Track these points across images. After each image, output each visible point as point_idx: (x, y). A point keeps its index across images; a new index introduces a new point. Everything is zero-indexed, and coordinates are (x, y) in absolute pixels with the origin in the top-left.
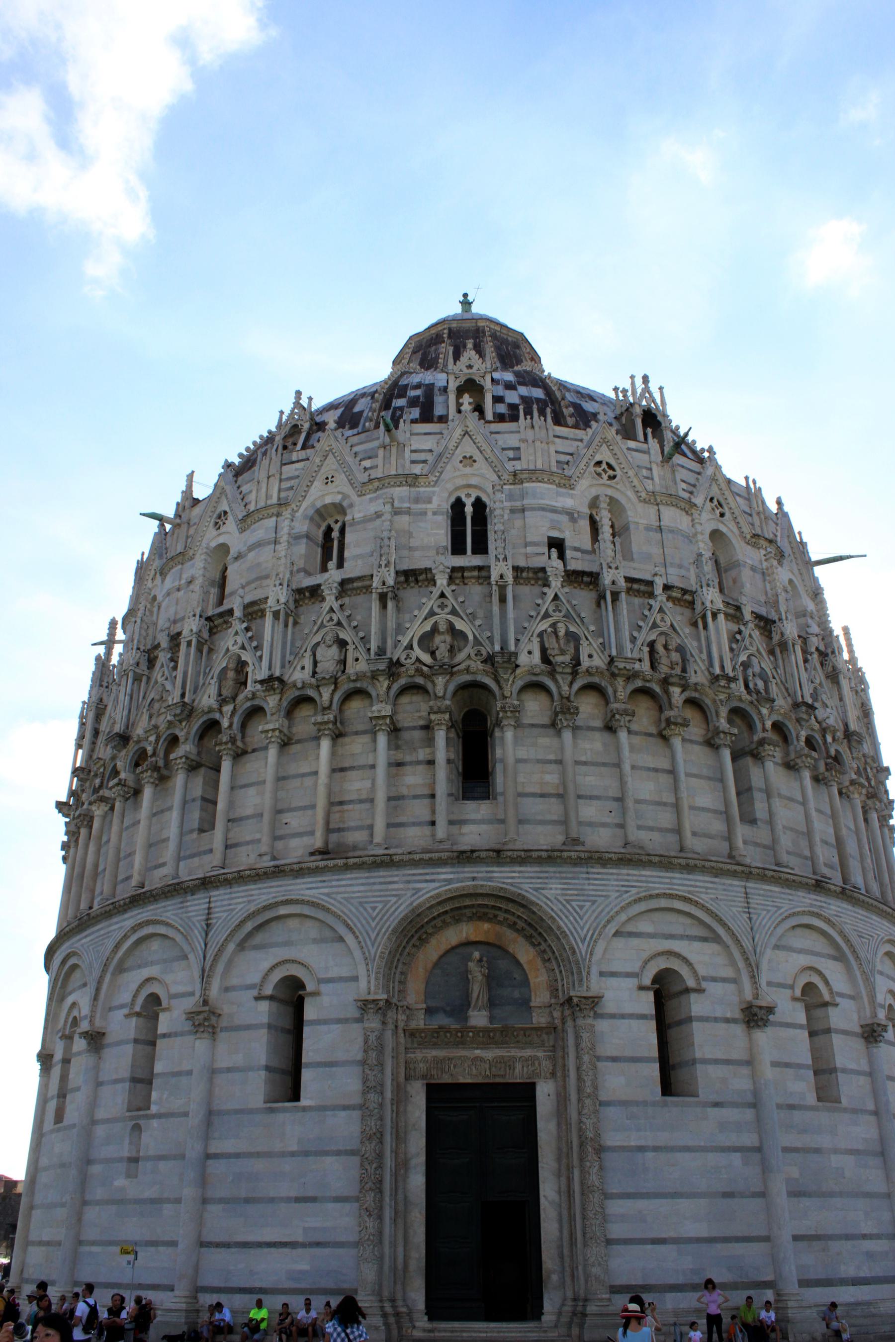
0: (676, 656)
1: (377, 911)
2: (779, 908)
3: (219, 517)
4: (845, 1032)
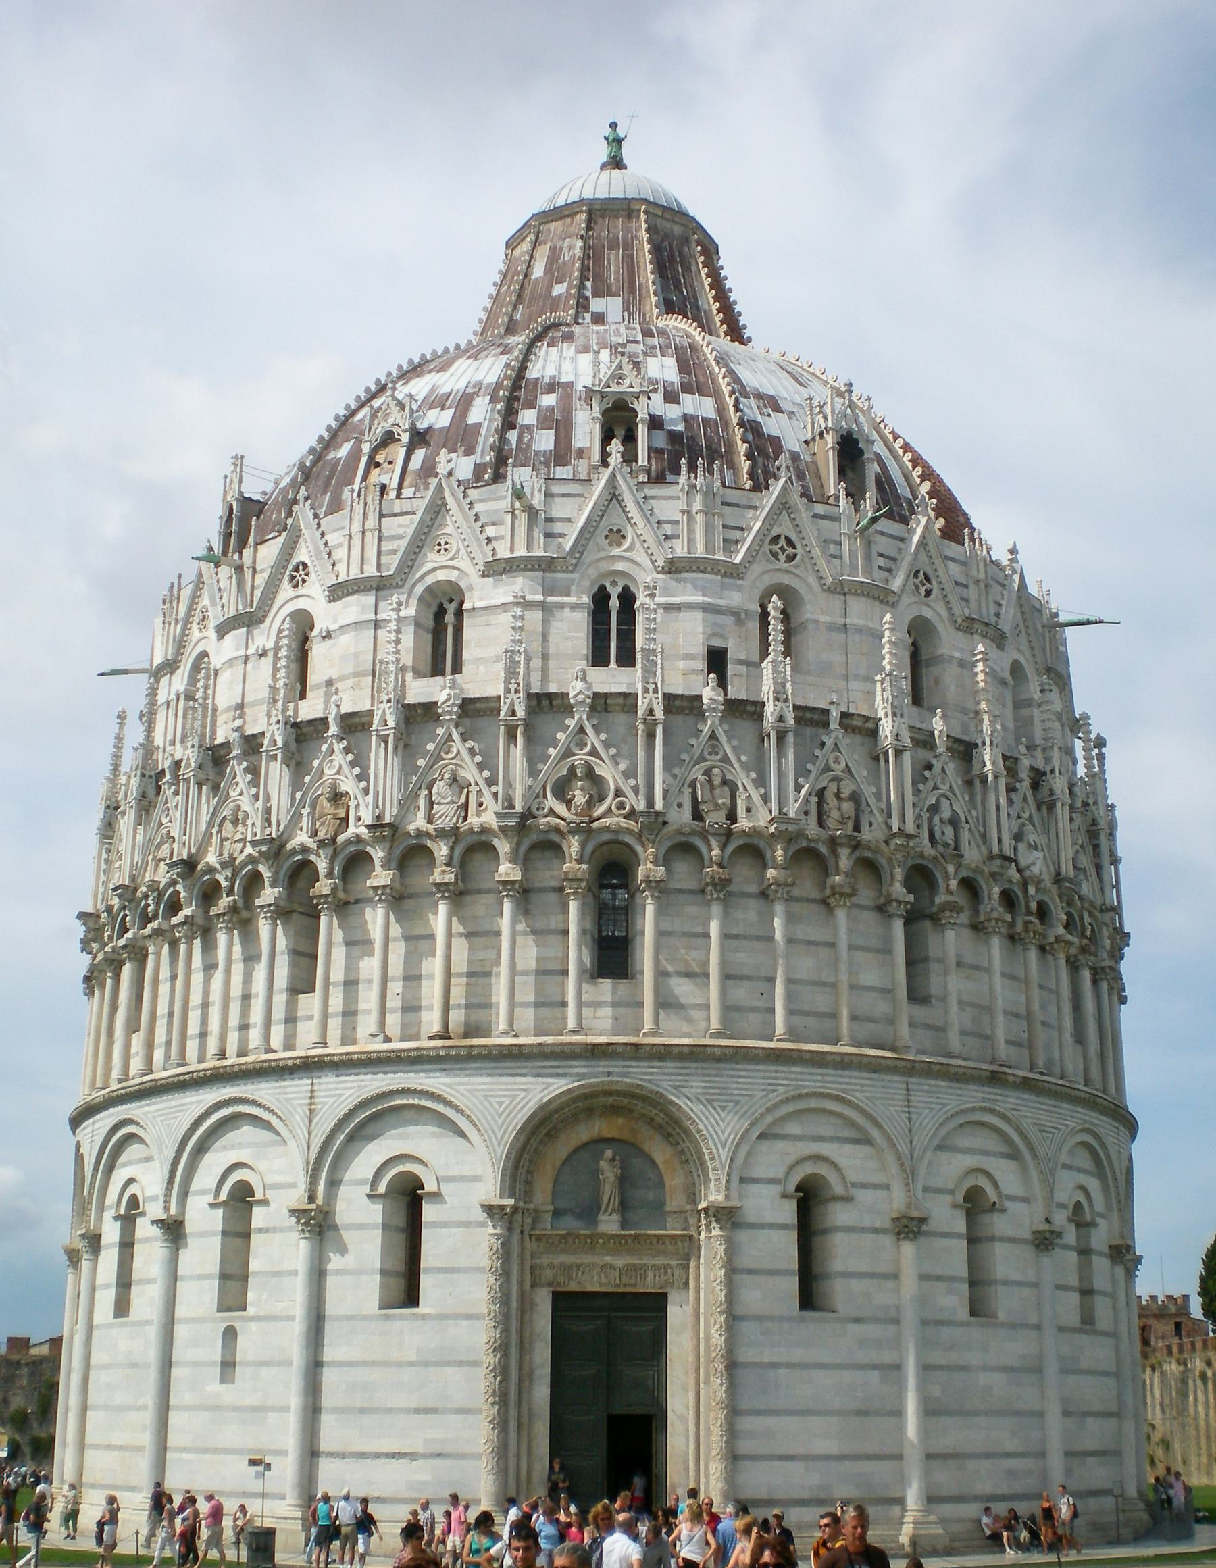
0: (848, 807)
2: (944, 1105)
3: (296, 569)
4: (1012, 1240)
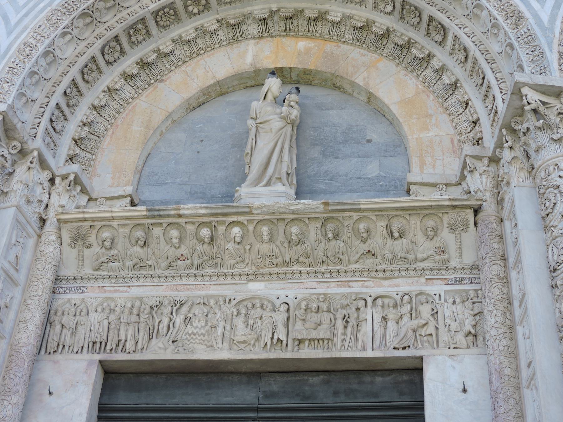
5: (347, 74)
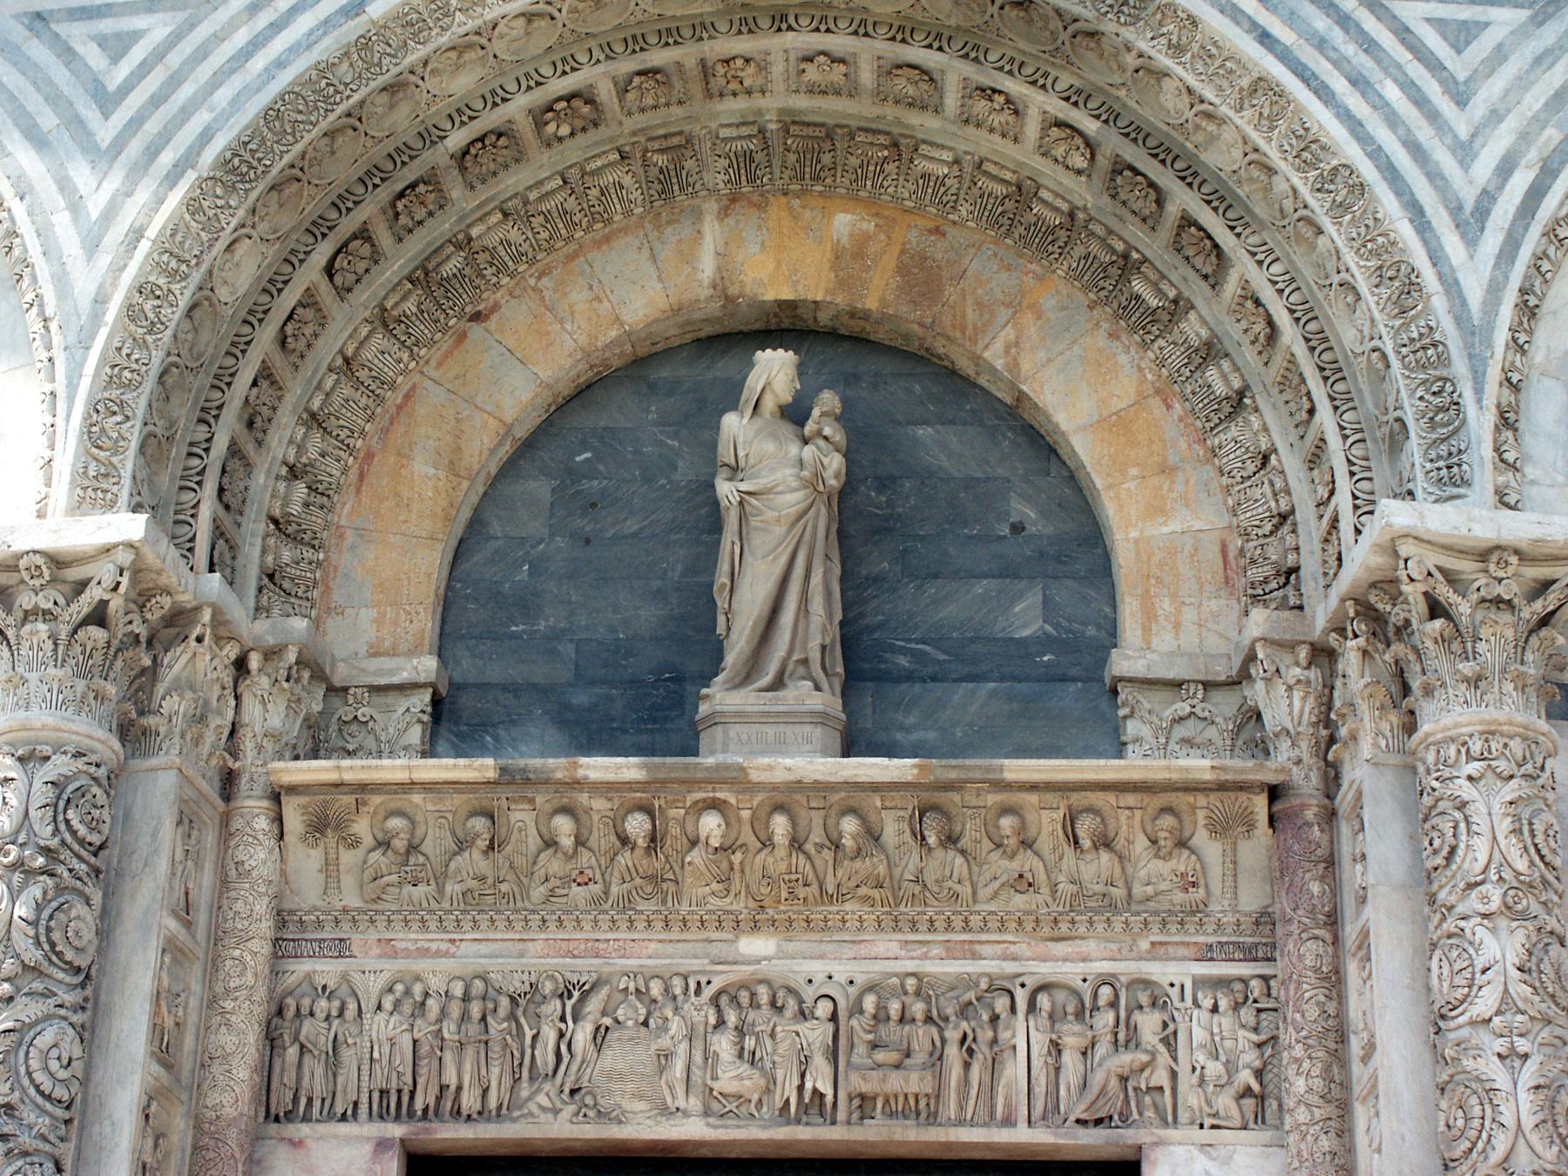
1: (138, 54)
5: (963, 329)
